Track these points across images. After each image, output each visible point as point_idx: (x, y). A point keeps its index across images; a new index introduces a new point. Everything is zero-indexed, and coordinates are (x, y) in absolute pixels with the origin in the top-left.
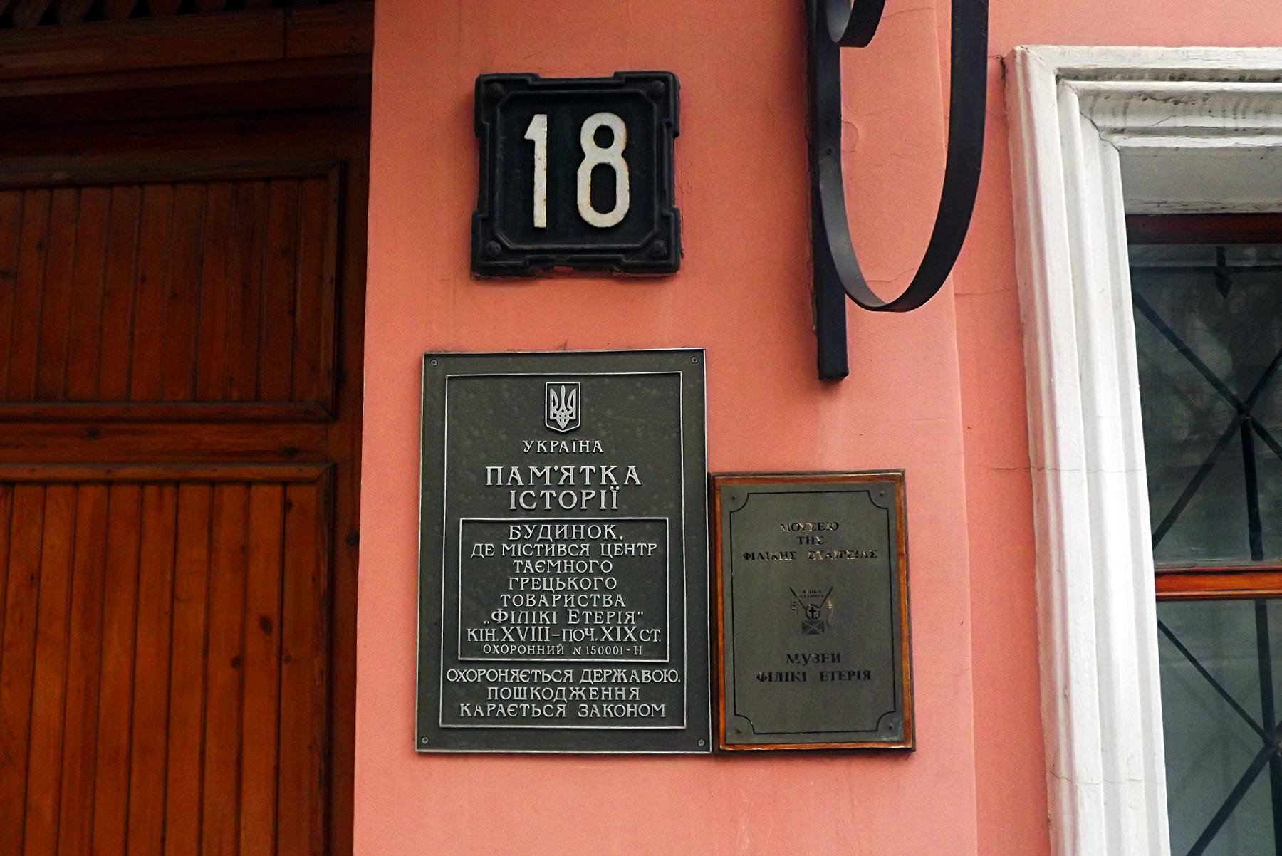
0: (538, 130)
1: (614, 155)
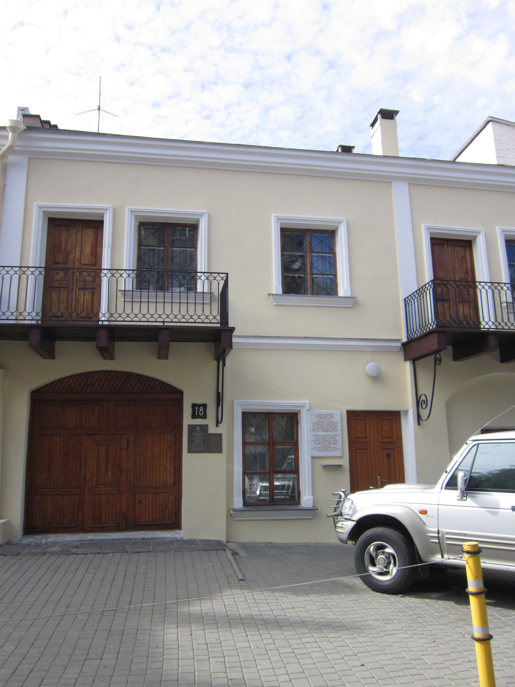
0: (196, 408)
1: (202, 410)
